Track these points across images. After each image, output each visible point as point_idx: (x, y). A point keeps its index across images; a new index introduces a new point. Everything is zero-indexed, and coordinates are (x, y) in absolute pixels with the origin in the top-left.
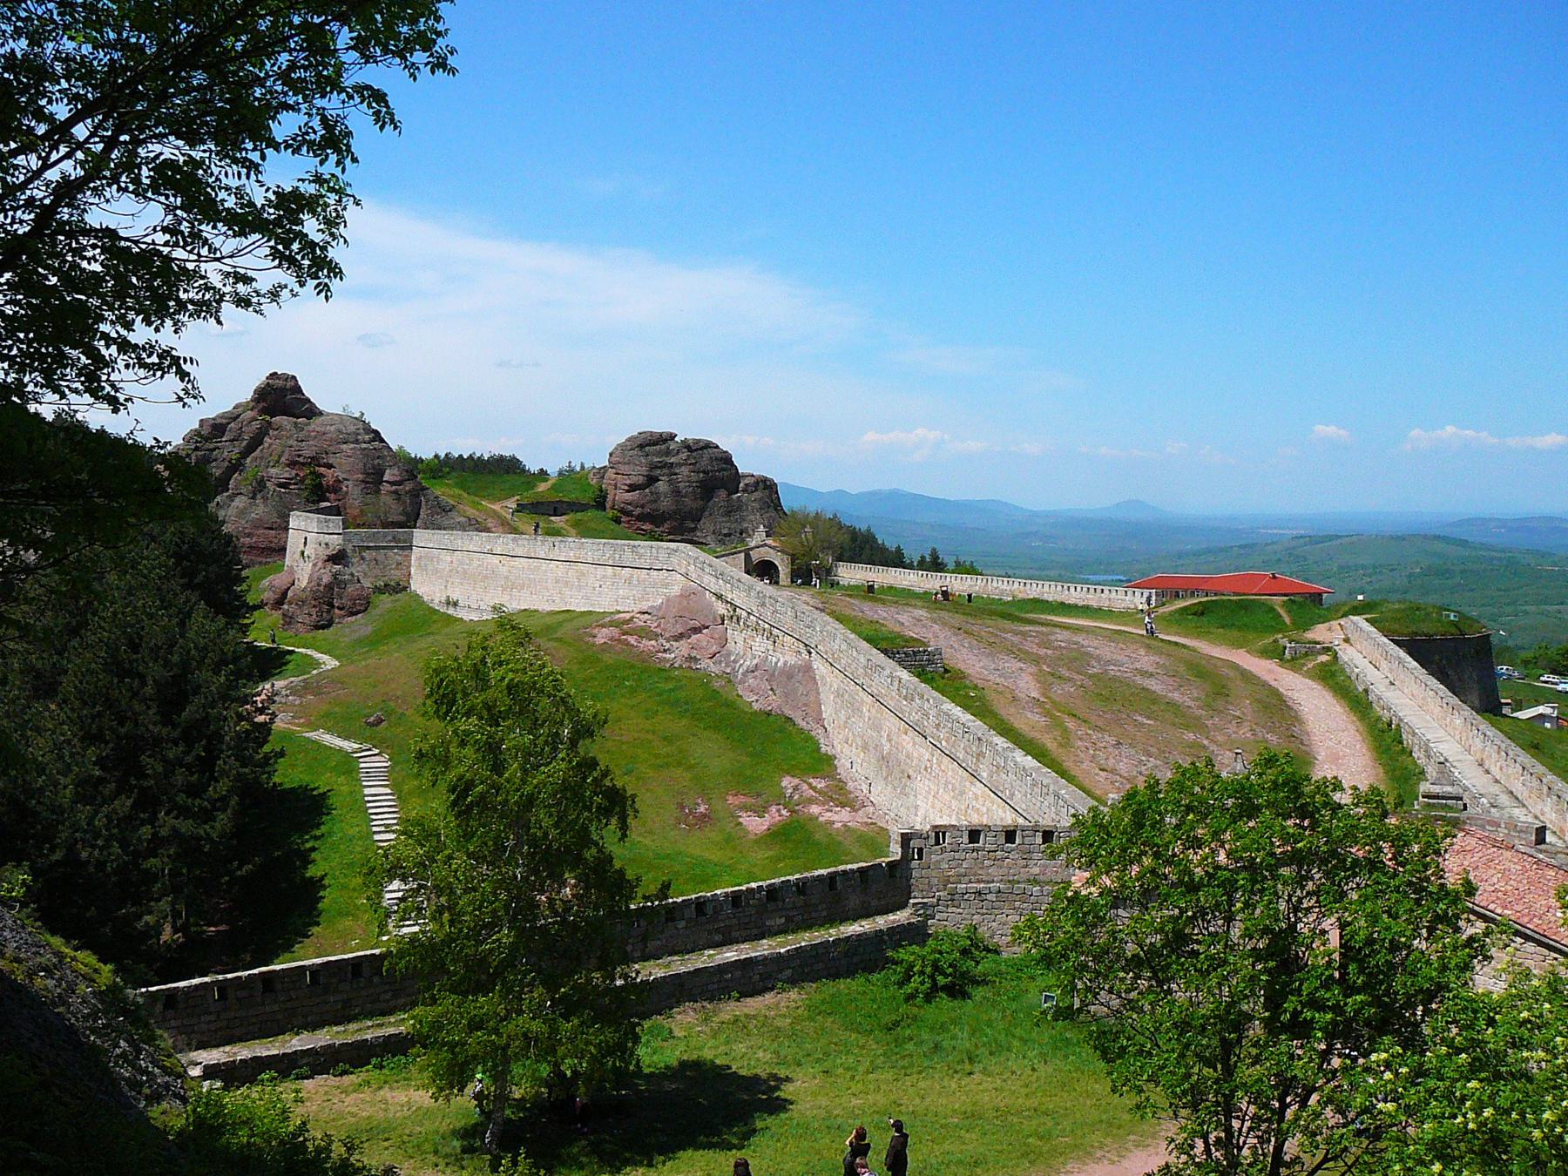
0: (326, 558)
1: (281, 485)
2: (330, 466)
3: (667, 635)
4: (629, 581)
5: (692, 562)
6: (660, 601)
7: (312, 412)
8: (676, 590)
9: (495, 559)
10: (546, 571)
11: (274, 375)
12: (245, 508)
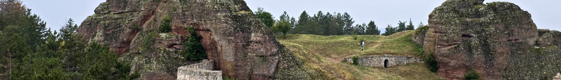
1: (171, 46)
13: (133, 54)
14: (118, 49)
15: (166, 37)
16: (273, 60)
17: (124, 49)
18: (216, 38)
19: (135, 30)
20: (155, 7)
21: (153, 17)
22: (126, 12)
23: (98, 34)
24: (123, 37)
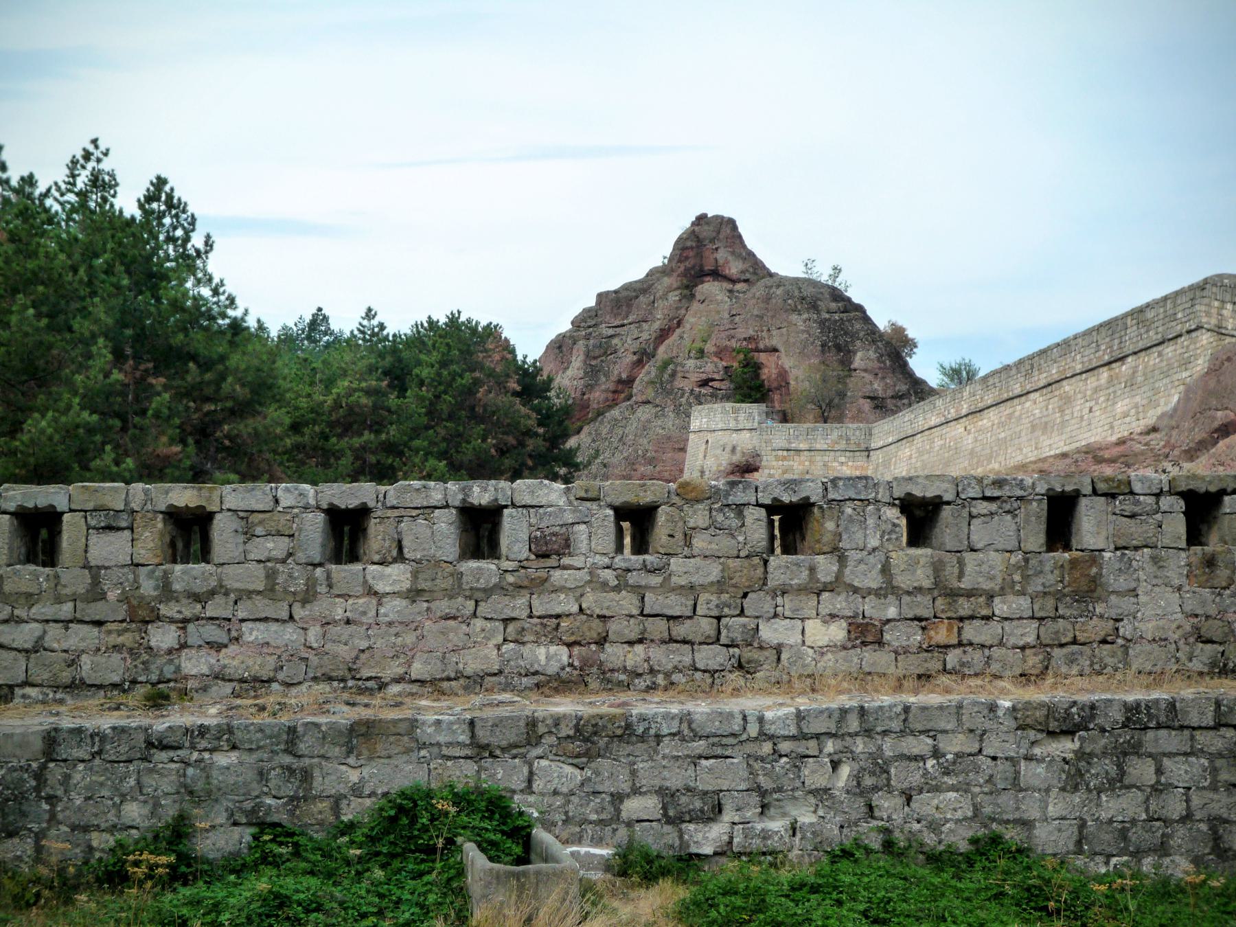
0: (730, 468)
2: (775, 350)
3: (1176, 452)
4: (1131, 384)
5: (1228, 297)
6: (1176, 398)
7: (756, 269)
8: (1201, 365)
9: (958, 429)
10: (1020, 418)
11: (701, 219)
12: (649, 421)
13: (636, 403)
14: (610, 396)
15: (696, 367)
16: (896, 406)
17: (623, 396)
18: (787, 362)
19: (643, 356)
20: (683, 311)
21: (678, 331)
22: (630, 324)
23: (573, 364)
24: (620, 368)
